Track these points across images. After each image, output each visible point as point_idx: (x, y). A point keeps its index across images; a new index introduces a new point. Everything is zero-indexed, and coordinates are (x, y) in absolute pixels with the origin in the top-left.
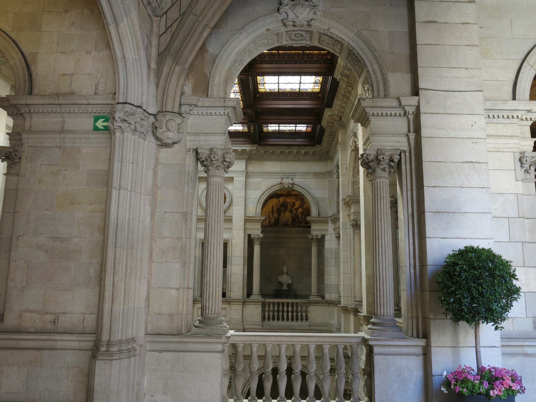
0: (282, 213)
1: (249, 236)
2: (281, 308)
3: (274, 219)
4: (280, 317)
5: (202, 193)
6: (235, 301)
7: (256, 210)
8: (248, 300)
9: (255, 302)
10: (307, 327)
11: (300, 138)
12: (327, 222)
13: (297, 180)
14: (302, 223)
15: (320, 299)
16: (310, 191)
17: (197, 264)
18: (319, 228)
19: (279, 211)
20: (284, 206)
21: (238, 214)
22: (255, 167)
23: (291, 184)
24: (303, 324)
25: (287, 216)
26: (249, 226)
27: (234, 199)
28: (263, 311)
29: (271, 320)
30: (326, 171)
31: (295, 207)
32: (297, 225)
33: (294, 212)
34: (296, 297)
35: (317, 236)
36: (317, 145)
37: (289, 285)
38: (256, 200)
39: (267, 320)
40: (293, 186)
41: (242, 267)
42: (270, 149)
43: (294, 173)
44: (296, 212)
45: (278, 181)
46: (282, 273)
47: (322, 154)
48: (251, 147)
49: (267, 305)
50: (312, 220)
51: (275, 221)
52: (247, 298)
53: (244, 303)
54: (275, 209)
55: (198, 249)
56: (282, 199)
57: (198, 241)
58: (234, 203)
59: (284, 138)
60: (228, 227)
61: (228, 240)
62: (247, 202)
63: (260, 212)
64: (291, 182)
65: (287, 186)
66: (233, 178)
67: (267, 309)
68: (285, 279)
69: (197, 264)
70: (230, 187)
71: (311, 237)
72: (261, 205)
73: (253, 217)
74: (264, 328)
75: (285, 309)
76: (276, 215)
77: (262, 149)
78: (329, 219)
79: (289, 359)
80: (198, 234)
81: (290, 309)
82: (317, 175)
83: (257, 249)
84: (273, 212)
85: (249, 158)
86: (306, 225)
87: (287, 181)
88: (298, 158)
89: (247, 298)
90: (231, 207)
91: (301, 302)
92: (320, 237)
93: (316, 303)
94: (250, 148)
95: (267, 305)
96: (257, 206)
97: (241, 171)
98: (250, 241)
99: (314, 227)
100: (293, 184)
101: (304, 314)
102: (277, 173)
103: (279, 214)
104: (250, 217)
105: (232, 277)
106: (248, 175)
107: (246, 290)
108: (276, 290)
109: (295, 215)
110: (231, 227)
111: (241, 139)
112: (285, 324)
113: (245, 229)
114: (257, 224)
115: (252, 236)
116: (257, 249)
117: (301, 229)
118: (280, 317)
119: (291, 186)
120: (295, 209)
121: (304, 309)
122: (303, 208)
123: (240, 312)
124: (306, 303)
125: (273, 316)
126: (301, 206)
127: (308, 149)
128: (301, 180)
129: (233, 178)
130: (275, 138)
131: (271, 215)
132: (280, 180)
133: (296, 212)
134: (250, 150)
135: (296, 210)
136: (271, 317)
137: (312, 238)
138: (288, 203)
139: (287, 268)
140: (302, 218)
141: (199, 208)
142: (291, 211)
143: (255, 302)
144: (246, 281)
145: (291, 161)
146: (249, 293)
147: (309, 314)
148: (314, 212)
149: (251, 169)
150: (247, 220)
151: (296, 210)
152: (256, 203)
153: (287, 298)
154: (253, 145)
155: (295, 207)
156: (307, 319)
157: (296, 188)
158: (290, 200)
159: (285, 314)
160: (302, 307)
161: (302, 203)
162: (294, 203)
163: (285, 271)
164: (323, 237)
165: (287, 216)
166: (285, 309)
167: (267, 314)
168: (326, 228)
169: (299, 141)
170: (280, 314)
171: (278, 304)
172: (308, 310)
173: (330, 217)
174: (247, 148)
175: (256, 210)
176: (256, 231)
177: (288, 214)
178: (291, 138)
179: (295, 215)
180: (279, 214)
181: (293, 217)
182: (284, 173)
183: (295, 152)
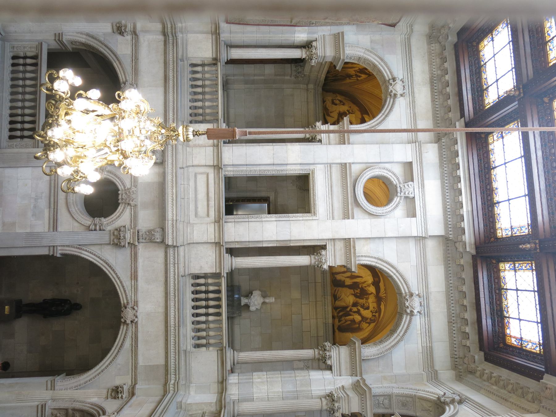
0: (352, 291)
1: (324, 247)
2: (212, 303)
3: (343, 279)
4: (198, 303)
5: (387, 170)
6: (220, 231)
7: (366, 256)
8: (223, 250)
10: (183, 347)
11: (493, 325)
12: (353, 373)
13: (418, 322)
14: (339, 322)
15: (229, 368)
16: (402, 343)
17: (275, 168)
18: (343, 361)
19: (354, 286)
20: (363, 294)
21: (359, 226)
22: (433, 251)
23: (412, 311)
24: (189, 341)
25: (348, 298)
26: (340, 246)
27: (381, 220)
28: (205, 276)
29: (193, 289)
30: (437, 367)
32: (336, 315)
33: (355, 309)
34: (230, 318)
35: (330, 357)
36: (482, 354)
37: (247, 306)
38: (380, 255)
39: (193, 281)
40: (407, 314)
41: (274, 238)
42: (468, 274)
43: (429, 316)
44: (354, 312)
45: (415, 291)
46: (264, 296)
47: (466, 360)
48: (470, 244)
49: (217, 281)
50: (355, 349)
51: (340, 281)
52: (227, 249)
53: (218, 244)
55: (298, 167)
56: (372, 289)
57: (312, 167)
58: (375, 221)
59: (491, 297)
60: (336, 214)
61: (315, 214)
62: (377, 240)
63: (362, 262)
64: (415, 311)
65: (407, 304)
66: (414, 215)
67: (210, 281)
68: (256, 301)
69: (275, 168)
71: (327, 348)
72: (373, 264)
73: (355, 253)
74: (181, 278)
75: (211, 311)
76: (348, 282)
77: (466, 261)
78: (358, 378)
79: (132, 322)
80: (322, 166)
82: (429, 353)
83: (303, 260)
84: (353, 277)
85: (449, 242)
86: (336, 328)
87: (415, 304)
88: (454, 321)
89: (227, 249)
90: (367, 216)
91: (222, 336)
92: (329, 362)
93: (223, 362)
94: (467, 241)
95: (217, 281)
96: (371, 257)
97: (426, 229)
98: (314, 249)
99: (344, 351)
100: (412, 314)
101: (204, 341)
102: (427, 287)
103: (350, 287)
104: (354, 247)
105: (258, 224)
106: (420, 239)
107: (237, 246)
108: (239, 287)
109: (351, 310)
110: (336, 217)
111: (482, 226)
112: (188, 311)
113: (334, 239)
114: (343, 258)
115: (323, 252)
116: (303, 260)
117: (330, 321)
118: (198, 303)
119: (408, 311)
120: (359, 310)
121: (212, 341)
122: (360, 322)
123: (204, 239)
124: (222, 343)
126: (364, 319)
127: (474, 337)
128: (419, 327)
129: (414, 215)
130: (489, 281)
131: (348, 274)
132: (417, 293)
133: (354, 312)
134: (465, 244)
135: (358, 312)
137: (325, 350)
138: (367, 299)
139: (271, 303)
140: (346, 321)
141: (363, 166)
142: (355, 304)
144: (251, 245)
145: (449, 308)
146: (233, 252)
147: (204, 349)
148: (369, 351)
149: (431, 245)
150: (348, 243)
151: (358, 312)
152: (376, 255)
153: (228, 305)
154: (473, 246)
155: (361, 310)
156: (198, 346)
157: (405, 319)
158: (371, 301)
159: (202, 311)
160: (214, 337)
161: (368, 321)
162: (368, 308)
163: (267, 300)
164: (330, 368)
165: (348, 298)
166: (211, 311)
167: (202, 281)
168: (343, 371)
169: (487, 322)
170: (203, 303)
171: (219, 292)
172: (211, 348)
173: (362, 379)
174: (468, 238)
175: (366, 256)
176: (332, 258)
177: (351, 299)
178: (492, 310)
179: (351, 310)
180: (350, 287)
181: (347, 307)
182: (428, 298)
183: (467, 316)
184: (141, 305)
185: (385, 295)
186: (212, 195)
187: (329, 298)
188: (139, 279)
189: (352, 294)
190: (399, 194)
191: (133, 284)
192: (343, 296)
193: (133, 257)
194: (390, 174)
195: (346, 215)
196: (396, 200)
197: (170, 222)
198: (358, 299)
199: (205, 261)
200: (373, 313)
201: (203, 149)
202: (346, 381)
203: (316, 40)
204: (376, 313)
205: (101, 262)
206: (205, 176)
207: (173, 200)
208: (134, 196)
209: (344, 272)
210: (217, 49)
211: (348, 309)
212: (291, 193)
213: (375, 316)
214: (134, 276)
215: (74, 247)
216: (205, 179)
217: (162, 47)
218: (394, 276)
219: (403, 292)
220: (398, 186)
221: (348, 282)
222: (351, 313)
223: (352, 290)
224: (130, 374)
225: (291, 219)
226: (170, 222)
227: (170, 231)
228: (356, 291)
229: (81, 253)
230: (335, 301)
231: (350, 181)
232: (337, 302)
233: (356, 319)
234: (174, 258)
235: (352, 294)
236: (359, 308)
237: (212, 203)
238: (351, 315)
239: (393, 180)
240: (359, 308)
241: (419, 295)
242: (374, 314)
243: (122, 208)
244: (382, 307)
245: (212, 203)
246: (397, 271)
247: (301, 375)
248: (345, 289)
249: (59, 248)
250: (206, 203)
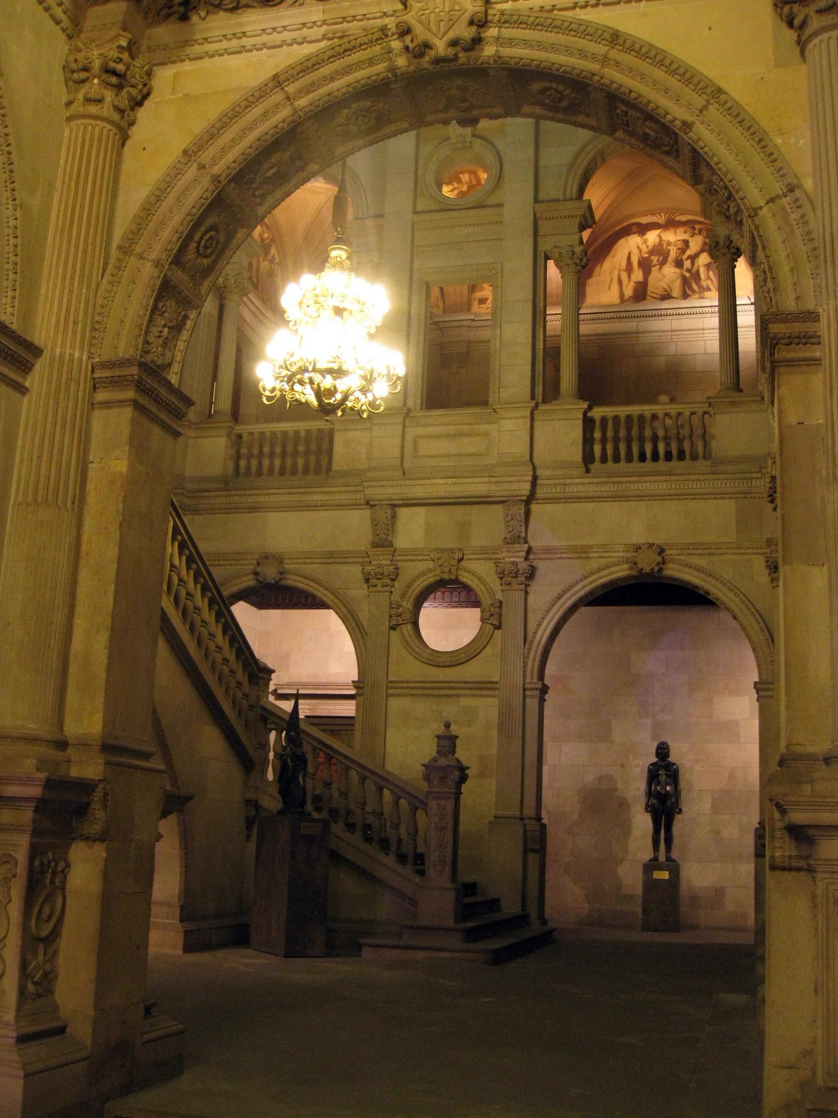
0: (655, 270)
3: (632, 285)
28: (588, 441)
31: (689, 252)
33: (687, 264)
44: (693, 264)
54: (635, 261)
56: (652, 237)
76: (638, 275)
84: (629, 269)
109: (689, 271)
120: (689, 257)
125: (616, 450)
131: (624, 276)
133: (693, 264)
135: (693, 258)
136: (609, 453)
138: (669, 244)
142: (679, 264)
155: (689, 252)
162: (686, 243)
167: (597, 449)
177: (670, 270)
179: (689, 271)
181: (684, 277)
185: (663, 215)
187: (665, 305)
189: (660, 268)
191: (596, 555)
192: (663, 284)
193: (550, 556)
197: (493, 487)
198: (670, 259)
200: (694, 234)
204: (694, 229)
205: (555, 608)
209: (620, 282)
211: (687, 275)
213: (700, 233)
214: (582, 552)
215: (529, 654)
221: (638, 275)
222: (694, 270)
223: (653, 269)
224: (752, 557)
228: (655, 262)
229: (539, 643)
230: (674, 298)
232: (674, 295)
233: (706, 262)
235: (660, 268)
236: (685, 256)
238: (698, 271)
240: (685, 256)
242: (697, 232)
243: (466, 574)
244: (683, 218)
248: (651, 281)
249: (528, 680)
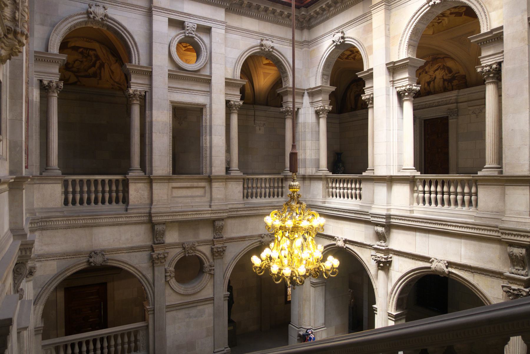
6: (219, 178)
9: (236, 179)
38: (234, 61)
61: (205, 105)
65: (267, 50)
70: (205, 38)
78: (306, 92)
81: (107, 189)
83: (235, 119)
100: (272, 48)
136: (249, 194)
143: (236, 179)
150: (229, 83)
173: (307, 90)
184: (260, 232)
186: (188, 184)
188: (244, 235)
190: (194, 36)
194: (176, 39)
195: (208, 81)
196: (197, 39)
197: (213, 215)
199: (236, 190)
201: (155, 191)
202: (306, 99)
203: (41, 81)
206: (175, 191)
207: (196, 214)
208: (191, 244)
210: (53, 179)
212: (188, 121)
216: (176, 190)
217: (48, 232)
218: (249, 54)
219: (259, 50)
220: (187, 35)
225: (208, 124)
226: (213, 215)
227: (218, 215)
231: (179, 72)
234: (233, 211)
237: (195, 184)
239: (181, 38)
241: (262, 40)
245: (195, 184)
246: (246, 51)
247: (300, 128)
250: (195, 189)
